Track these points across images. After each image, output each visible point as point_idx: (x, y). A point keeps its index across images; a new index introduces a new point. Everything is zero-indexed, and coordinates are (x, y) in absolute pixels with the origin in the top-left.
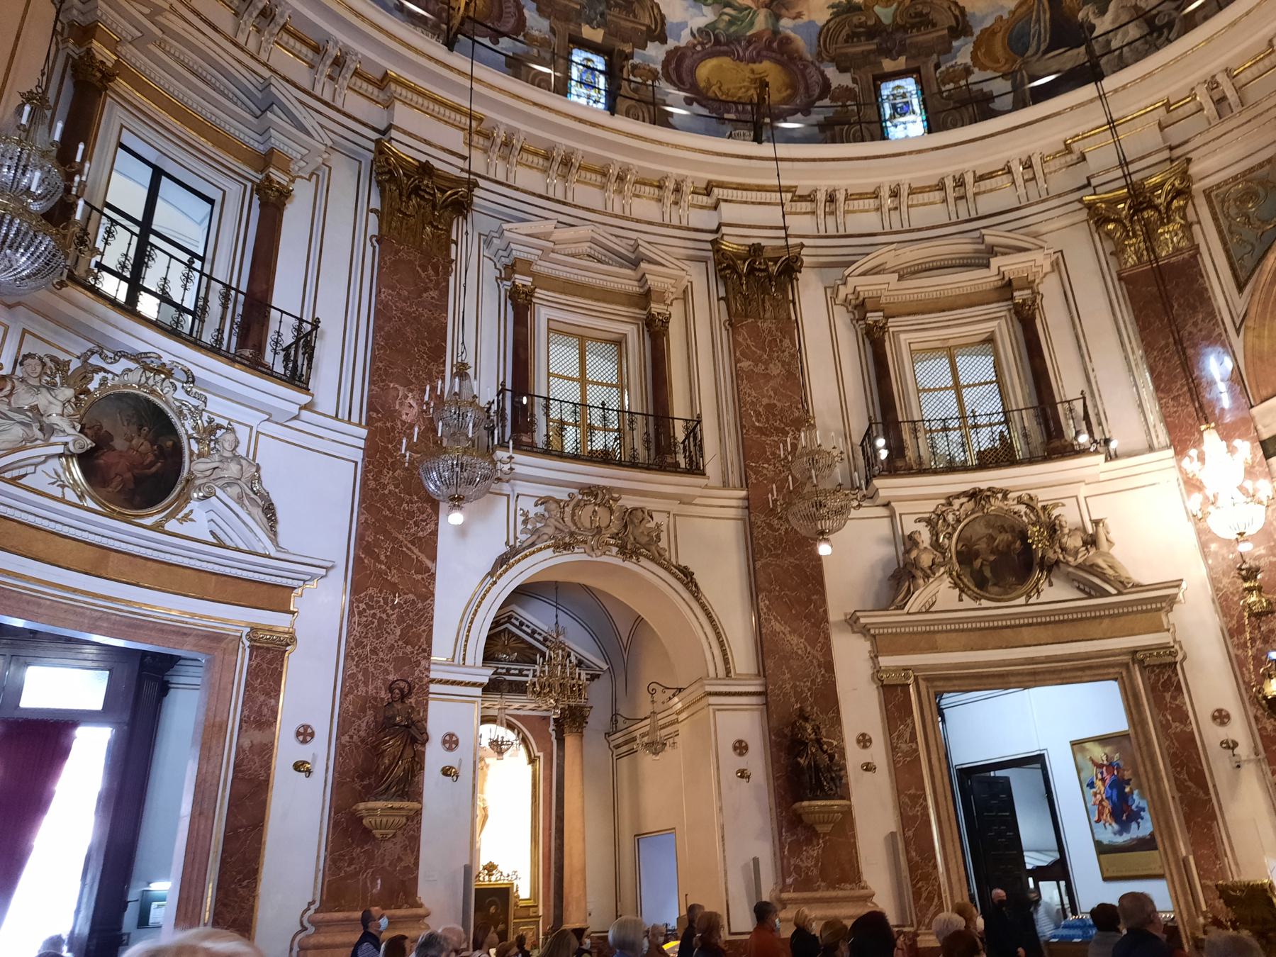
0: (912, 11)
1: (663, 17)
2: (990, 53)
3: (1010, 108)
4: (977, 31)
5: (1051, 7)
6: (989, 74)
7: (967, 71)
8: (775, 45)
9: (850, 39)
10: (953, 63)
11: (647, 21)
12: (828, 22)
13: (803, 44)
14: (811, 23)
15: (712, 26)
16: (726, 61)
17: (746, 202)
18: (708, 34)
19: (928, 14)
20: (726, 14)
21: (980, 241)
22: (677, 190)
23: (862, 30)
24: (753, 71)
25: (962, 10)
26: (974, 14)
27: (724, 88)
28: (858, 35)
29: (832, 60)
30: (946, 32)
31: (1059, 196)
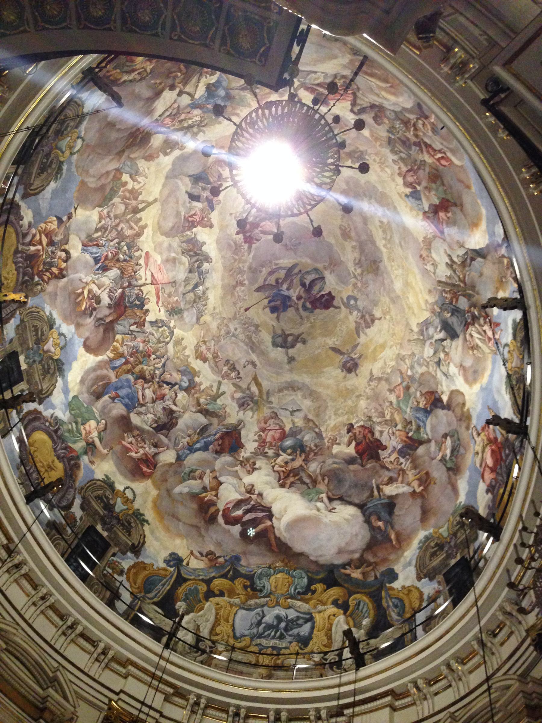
0: (128, 518)
1: (51, 394)
2: (136, 574)
3: (121, 612)
4: (141, 559)
5: (172, 586)
6: (127, 585)
7: (121, 573)
8: (72, 462)
9: (99, 498)
10: (120, 561)
11: (45, 387)
12: (99, 480)
13: (81, 477)
14: (93, 472)
15: (63, 423)
16: (49, 443)
18: (57, 424)
19: (132, 527)
20: (72, 425)
21: (53, 670)
23: (105, 500)
24: (53, 461)
25: (144, 542)
26: (146, 550)
27: (36, 454)
28: (102, 501)
29: (83, 498)
30: (130, 544)
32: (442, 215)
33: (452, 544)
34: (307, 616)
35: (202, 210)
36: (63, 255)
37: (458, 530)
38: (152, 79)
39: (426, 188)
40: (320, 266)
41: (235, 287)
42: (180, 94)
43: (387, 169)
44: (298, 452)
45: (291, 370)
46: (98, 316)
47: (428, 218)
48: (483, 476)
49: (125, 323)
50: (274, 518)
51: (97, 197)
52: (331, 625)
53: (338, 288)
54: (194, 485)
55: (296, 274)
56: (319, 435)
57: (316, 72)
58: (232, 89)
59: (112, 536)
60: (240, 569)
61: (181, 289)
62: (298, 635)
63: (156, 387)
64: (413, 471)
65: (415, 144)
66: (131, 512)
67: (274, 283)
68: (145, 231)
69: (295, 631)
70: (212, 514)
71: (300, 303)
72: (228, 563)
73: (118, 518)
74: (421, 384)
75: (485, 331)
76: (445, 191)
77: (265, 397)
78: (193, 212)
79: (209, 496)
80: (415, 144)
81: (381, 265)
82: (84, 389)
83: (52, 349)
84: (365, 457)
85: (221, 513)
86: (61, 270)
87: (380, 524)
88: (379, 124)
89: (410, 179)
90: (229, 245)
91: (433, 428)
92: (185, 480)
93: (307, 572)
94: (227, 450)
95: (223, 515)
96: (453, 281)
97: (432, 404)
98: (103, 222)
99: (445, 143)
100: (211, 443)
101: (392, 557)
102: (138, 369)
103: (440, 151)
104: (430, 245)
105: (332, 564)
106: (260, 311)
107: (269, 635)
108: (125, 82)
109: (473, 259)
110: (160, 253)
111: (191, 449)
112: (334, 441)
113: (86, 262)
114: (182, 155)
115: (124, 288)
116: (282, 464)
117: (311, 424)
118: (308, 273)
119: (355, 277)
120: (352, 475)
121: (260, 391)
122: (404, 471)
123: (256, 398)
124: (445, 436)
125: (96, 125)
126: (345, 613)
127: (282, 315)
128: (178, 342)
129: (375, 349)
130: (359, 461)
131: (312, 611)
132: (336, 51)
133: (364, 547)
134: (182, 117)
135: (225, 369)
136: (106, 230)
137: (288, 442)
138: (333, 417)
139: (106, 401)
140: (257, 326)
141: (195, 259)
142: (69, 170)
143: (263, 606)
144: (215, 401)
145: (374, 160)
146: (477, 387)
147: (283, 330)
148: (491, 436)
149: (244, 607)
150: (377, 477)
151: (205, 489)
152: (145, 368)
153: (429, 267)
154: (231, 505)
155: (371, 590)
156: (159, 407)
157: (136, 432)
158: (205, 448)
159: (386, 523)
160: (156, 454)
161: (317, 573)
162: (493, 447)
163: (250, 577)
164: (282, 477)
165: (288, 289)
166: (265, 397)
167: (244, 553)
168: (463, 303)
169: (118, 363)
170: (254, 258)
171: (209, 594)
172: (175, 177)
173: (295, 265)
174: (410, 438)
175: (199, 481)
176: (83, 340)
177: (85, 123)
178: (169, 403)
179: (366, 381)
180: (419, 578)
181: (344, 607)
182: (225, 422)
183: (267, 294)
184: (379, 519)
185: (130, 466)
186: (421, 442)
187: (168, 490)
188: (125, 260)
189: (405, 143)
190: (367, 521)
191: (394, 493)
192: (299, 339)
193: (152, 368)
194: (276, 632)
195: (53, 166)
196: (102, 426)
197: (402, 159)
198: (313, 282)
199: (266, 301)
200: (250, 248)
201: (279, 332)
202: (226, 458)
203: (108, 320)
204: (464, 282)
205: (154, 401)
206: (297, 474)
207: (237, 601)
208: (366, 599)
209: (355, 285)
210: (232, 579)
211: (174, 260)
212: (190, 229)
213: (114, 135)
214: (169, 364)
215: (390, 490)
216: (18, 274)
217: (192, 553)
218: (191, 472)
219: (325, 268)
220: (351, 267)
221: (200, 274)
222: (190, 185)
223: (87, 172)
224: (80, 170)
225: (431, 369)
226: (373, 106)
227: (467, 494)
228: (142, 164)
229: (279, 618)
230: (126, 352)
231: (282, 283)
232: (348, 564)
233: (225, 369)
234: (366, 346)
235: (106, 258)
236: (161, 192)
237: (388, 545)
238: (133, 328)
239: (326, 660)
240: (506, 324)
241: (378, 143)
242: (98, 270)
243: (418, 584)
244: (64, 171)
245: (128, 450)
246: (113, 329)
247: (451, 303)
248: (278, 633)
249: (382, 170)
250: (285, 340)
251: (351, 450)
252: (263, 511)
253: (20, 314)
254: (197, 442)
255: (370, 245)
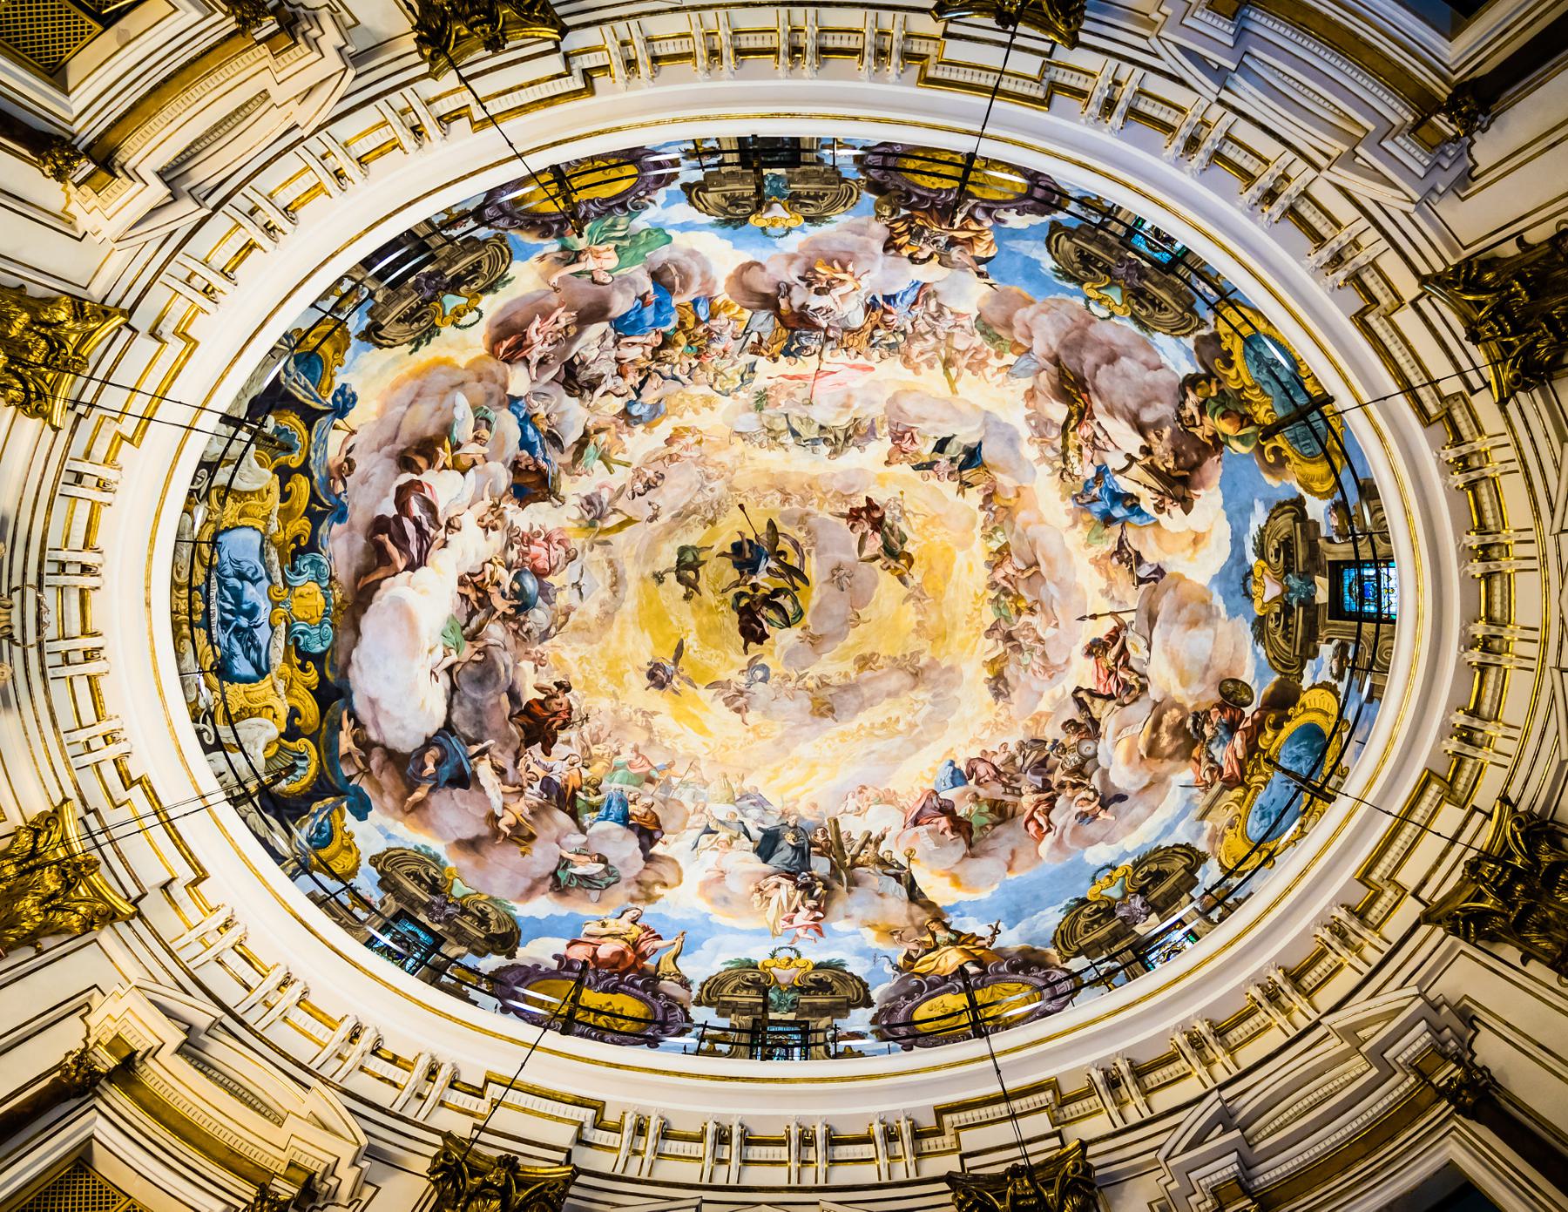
0: (429, 318)
1: (691, 203)
5: (302, 403)
8: (556, 227)
9: (477, 266)
11: (708, 196)
14: (525, 258)
15: (632, 216)
17: (531, 84)
18: (636, 208)
22: (631, 64)
25: (380, 346)
26: (368, 350)
28: (469, 273)
29: (485, 242)
31: (146, 290)
32: (944, 822)
33: (449, 910)
34: (263, 666)
35: (917, 453)
36: (922, 255)
37: (471, 914)
38: (1174, 431)
39: (977, 796)
40: (807, 619)
41: (782, 491)
42: (1131, 459)
43: (988, 733)
44: (516, 602)
45: (643, 579)
46: (795, 289)
47: (929, 798)
48: (574, 943)
49: (768, 326)
50: (409, 573)
51: (995, 316)
52: (259, 715)
53: (777, 650)
54: (464, 429)
55: (793, 584)
56: (545, 636)
57: (1149, 649)
58: (1123, 526)
59: (404, 291)
60: (326, 523)
61: (795, 412)
62: (232, 655)
63: (642, 365)
64: (527, 811)
65: (1046, 782)
66: (438, 321)
67: (778, 548)
68: (910, 372)
69: (237, 649)
70: (415, 462)
71: (747, 589)
72: (333, 498)
73: (433, 299)
74: (664, 802)
75: (797, 910)
76: (983, 827)
77: (601, 538)
78: (917, 439)
79: (444, 455)
80: (1046, 782)
81: (828, 721)
82: (677, 255)
83: (769, 215)
84: (524, 720)
85: (415, 477)
86: (899, 248)
87: (431, 768)
88: (1064, 726)
89: (982, 769)
90: (853, 486)
91: (605, 835)
92: (475, 412)
93: (330, 647)
94: (518, 481)
95: (412, 482)
96: (847, 847)
97: (641, 827)
98: (949, 316)
99: (1067, 832)
100: (532, 453)
101: (389, 801)
102: (682, 338)
103: (1049, 822)
104: (889, 802)
105: (351, 693)
106: (738, 528)
107: (225, 600)
108: (1186, 396)
109: (897, 877)
110: (865, 387)
111: (527, 420)
112: (540, 662)
113: (893, 284)
114: (1019, 438)
115: (826, 331)
116: (496, 577)
117: (561, 619)
118: (795, 601)
119: (801, 677)
120: (493, 701)
121: (609, 530)
122: (521, 793)
123: (599, 523)
124: (602, 859)
125: (1120, 340)
126: (282, 735)
127: (729, 561)
128: (708, 402)
129: (694, 717)
130: (517, 711)
131: (273, 672)
132: (1196, 688)
133: (389, 746)
134: (1085, 451)
135: (650, 474)
136: (934, 319)
137: (530, 584)
138: (576, 656)
139: (643, 286)
140: (713, 522)
141: (841, 436)
142: (1064, 289)
143: (270, 578)
144: (600, 458)
145: (998, 715)
146: (703, 906)
147: (704, 562)
148: (643, 947)
149: (266, 539)
150: (499, 746)
151: (457, 446)
152: (679, 350)
153: (852, 804)
154: (427, 494)
155: (329, 775)
156: (608, 368)
157: (573, 331)
158: (525, 444)
159: (435, 777)
160: (527, 362)
161: (333, 668)
162: (629, 954)
163: (313, 546)
164: (476, 579)
165: (768, 570)
166: (601, 538)
167: (351, 527)
168: (821, 866)
169: (703, 311)
170: (824, 522)
171: (284, 473)
172: (985, 424)
173: (806, 581)
174: (574, 796)
175: (471, 436)
176: (763, 262)
177: (1135, 328)
178: (608, 384)
179: (641, 705)
180: (374, 861)
181: (292, 733)
182: (563, 476)
183: (764, 538)
184: (437, 764)
185: (518, 319)
186: (574, 815)
187: (462, 383)
188: (872, 337)
189: (1041, 766)
190: (429, 743)
191: (482, 782)
192: (692, 587)
193: (677, 360)
194: (230, 612)
195: (1081, 273)
196: (601, 277)
197: (1013, 759)
198: (780, 609)
199: (752, 537)
200: (842, 515)
201: (702, 557)
202: (504, 478)
203: (783, 303)
204: (854, 865)
205: (617, 360)
206: (482, 606)
207: (274, 528)
208: (312, 770)
209: (787, 678)
210: (309, 513)
211: (847, 406)
212: (891, 432)
213: (1090, 359)
214: (672, 386)
215: (485, 771)
216: (929, 190)
217: (353, 432)
218: (488, 422)
219: (804, 628)
220: (815, 671)
221: (814, 441)
222: (966, 442)
223: (1045, 312)
224: (1054, 304)
225: (693, 819)
226: (1096, 723)
227: (532, 919)
228: (1026, 383)
229: (252, 612)
230: (713, 322)
231: (778, 561)
232: (358, 724)
233: (650, 474)
234: (696, 701)
235: (886, 312)
236: (966, 401)
237: (404, 790)
238: (754, 337)
239: (204, 722)
240: (828, 948)
241: (1030, 723)
242: (874, 298)
243: (365, 863)
244: (1064, 283)
245: (545, 316)
246: (763, 308)
247: (812, 844)
248: (229, 617)
249: (986, 725)
250: (689, 567)
251: (529, 694)
252: (420, 552)
253: (857, 181)
254: (536, 431)
255: (856, 702)
